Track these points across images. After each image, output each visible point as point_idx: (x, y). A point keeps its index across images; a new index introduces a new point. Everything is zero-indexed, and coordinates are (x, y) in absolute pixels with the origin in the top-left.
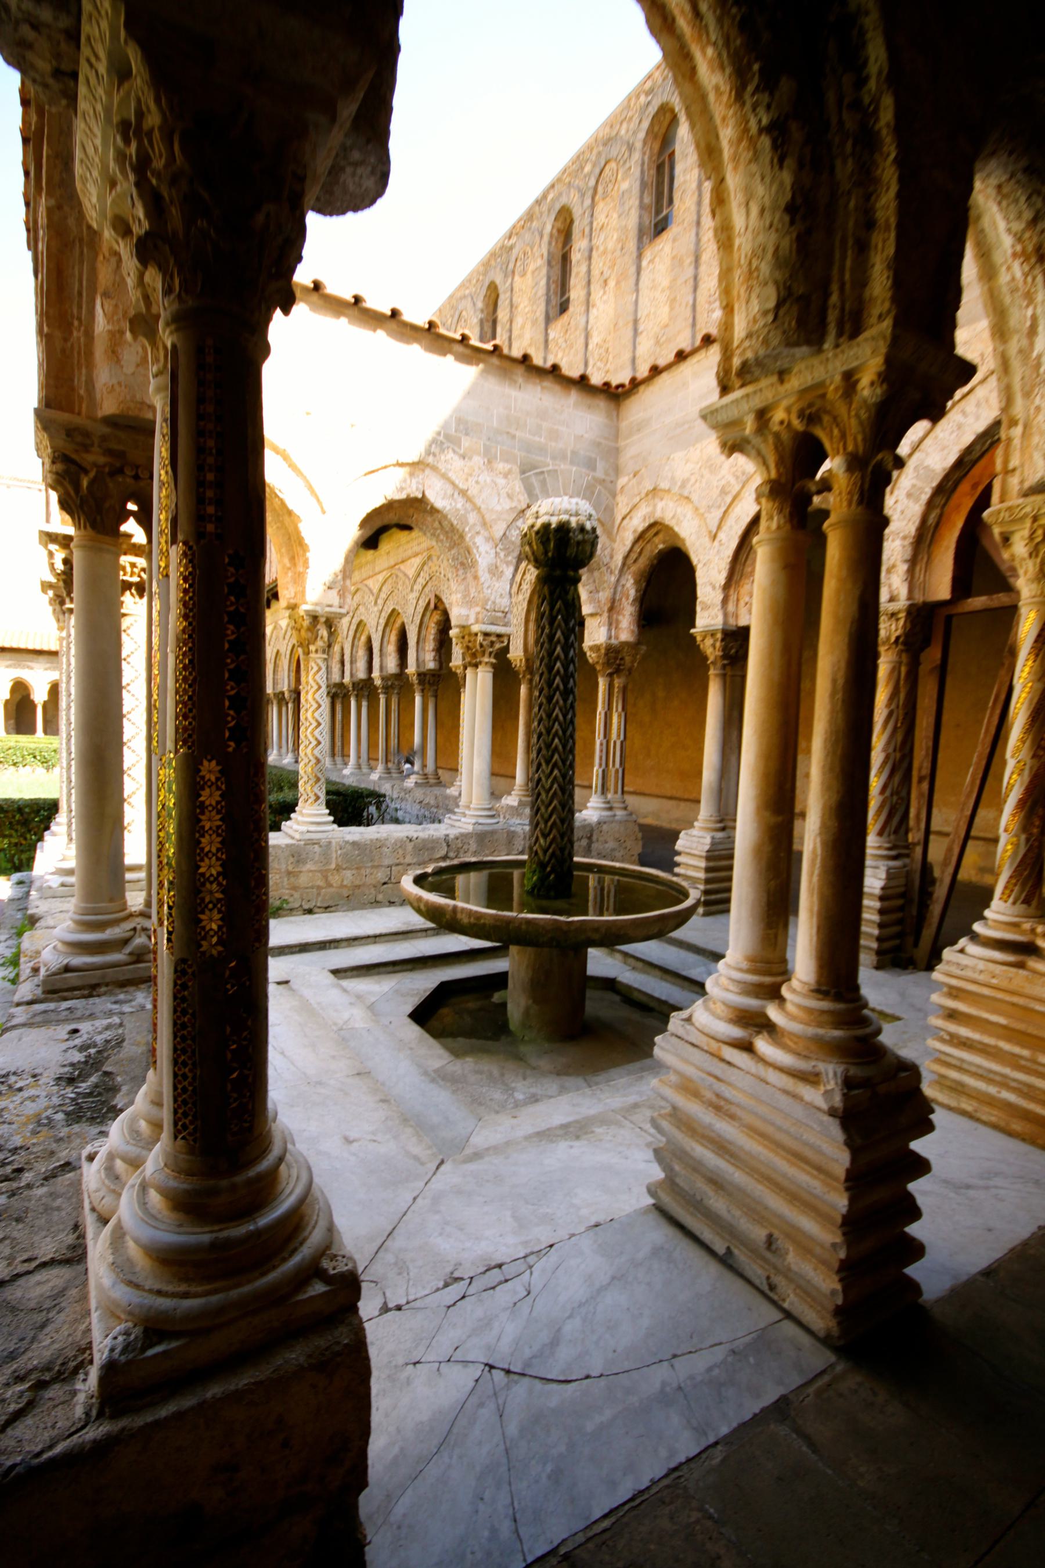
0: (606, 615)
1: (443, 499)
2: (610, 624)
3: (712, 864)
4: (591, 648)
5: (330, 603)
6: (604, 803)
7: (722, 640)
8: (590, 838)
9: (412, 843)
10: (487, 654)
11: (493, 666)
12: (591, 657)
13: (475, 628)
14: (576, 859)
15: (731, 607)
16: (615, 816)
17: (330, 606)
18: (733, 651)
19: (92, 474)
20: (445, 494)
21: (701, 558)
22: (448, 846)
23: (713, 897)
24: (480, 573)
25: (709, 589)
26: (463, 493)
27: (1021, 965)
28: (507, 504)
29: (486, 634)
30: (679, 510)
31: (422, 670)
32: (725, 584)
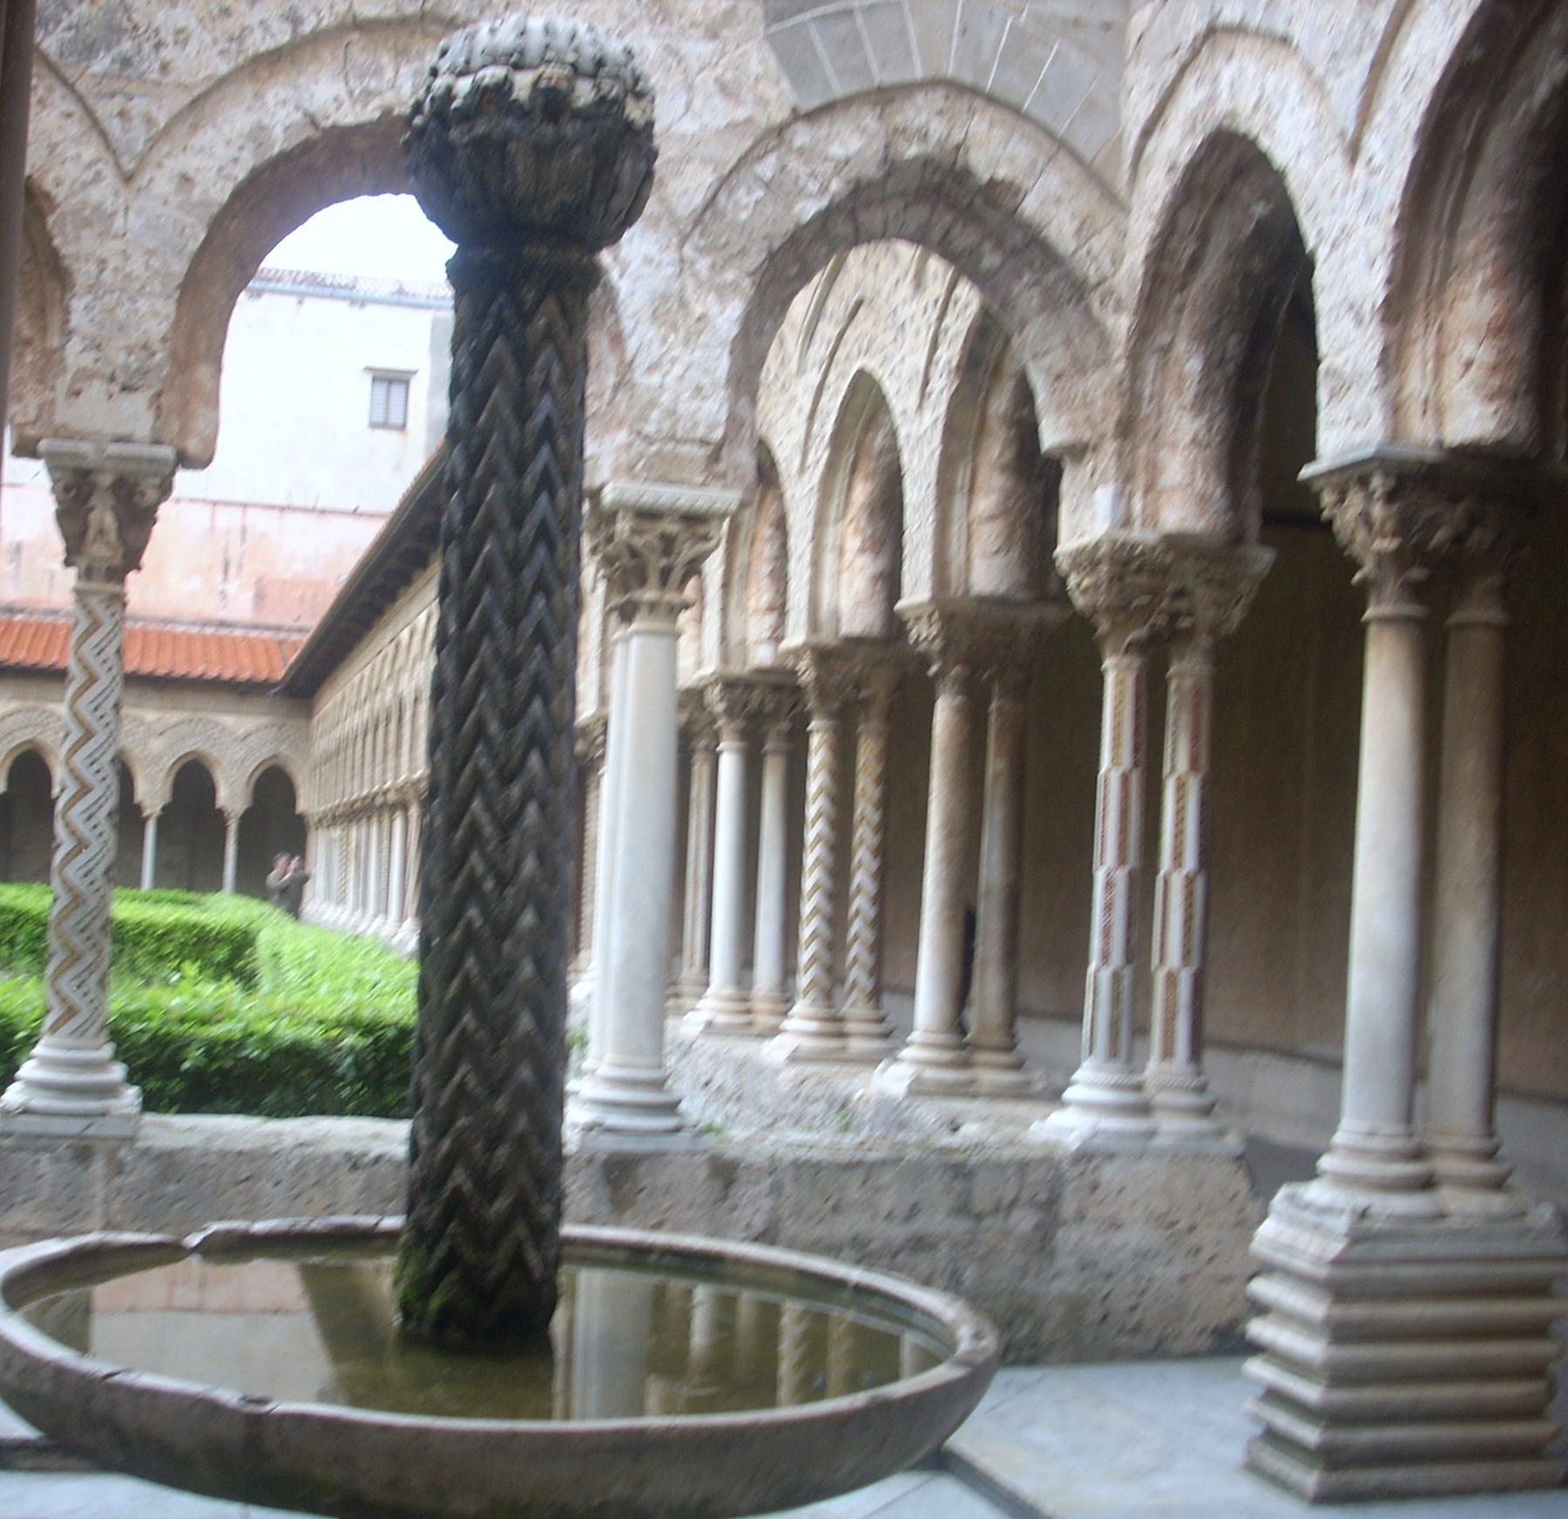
0: (1110, 447)
2: (1127, 478)
3: (1358, 1312)
5: (123, 430)
6: (1117, 1087)
7: (1390, 497)
8: (1050, 1204)
9: (361, 1176)
10: (654, 578)
14: (569, 1229)
15: (1416, 382)
16: (1152, 1134)
18: (1441, 536)
21: (1326, 223)
23: (1366, 1437)
24: (627, 324)
25: (1347, 323)
28: (718, 114)
29: (646, 515)
30: (1271, 80)
31: (736, 669)
32: (1387, 302)
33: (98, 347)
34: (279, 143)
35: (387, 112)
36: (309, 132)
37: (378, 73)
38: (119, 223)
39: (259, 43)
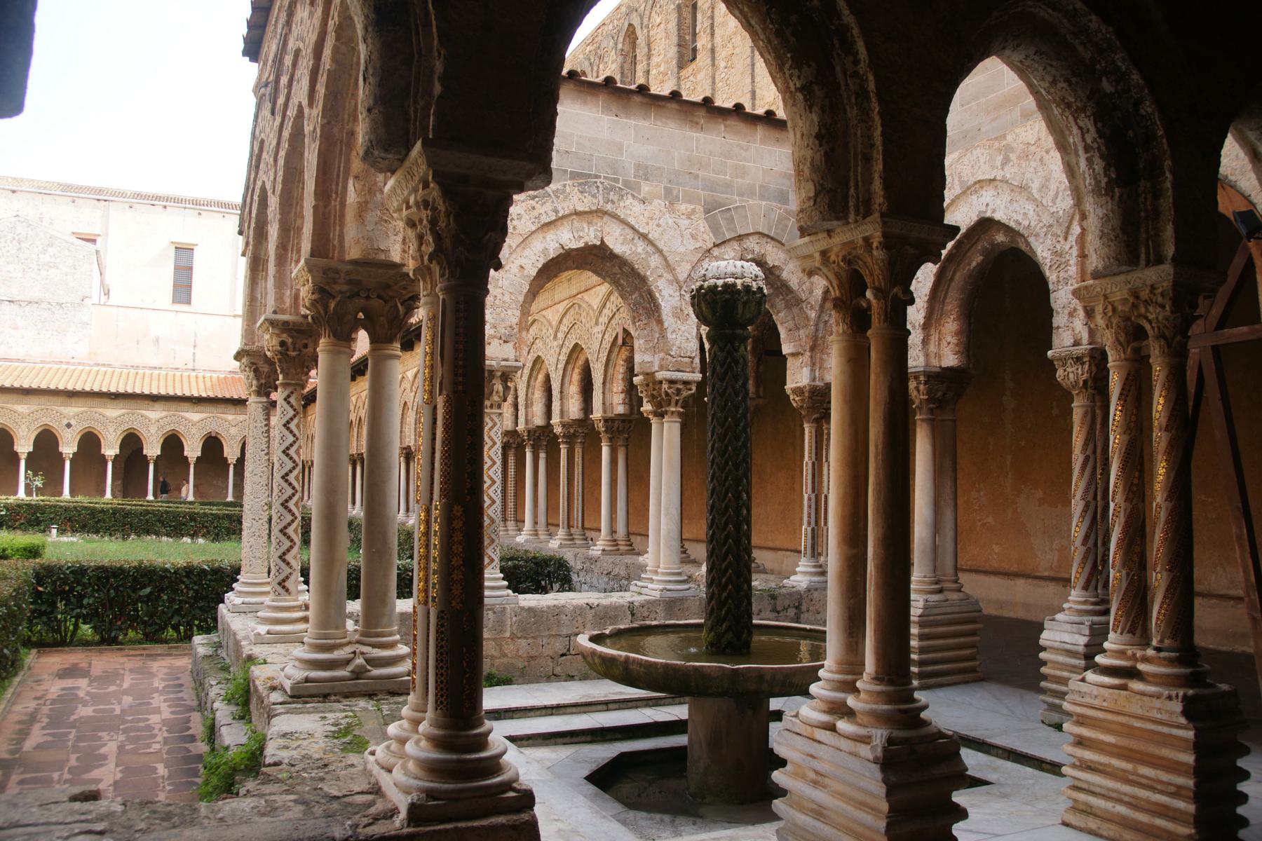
0: (808, 354)
1: (622, 244)
2: (813, 364)
3: (926, 630)
4: (795, 391)
5: (506, 357)
6: (815, 566)
7: (926, 383)
8: (798, 608)
9: (593, 611)
10: (673, 403)
11: (680, 414)
12: (795, 400)
13: (660, 375)
15: (932, 348)
17: (506, 360)
18: (939, 394)
19: (338, 299)
20: (625, 239)
22: (633, 615)
23: (930, 668)
24: (664, 317)
26: (644, 237)
27: (1123, 687)
28: (692, 245)
29: (672, 382)
31: (609, 415)
32: (924, 323)
33: (495, 327)
34: (552, 255)
35: (586, 243)
36: (562, 251)
37: (582, 230)
38: (500, 282)
39: (545, 219)
